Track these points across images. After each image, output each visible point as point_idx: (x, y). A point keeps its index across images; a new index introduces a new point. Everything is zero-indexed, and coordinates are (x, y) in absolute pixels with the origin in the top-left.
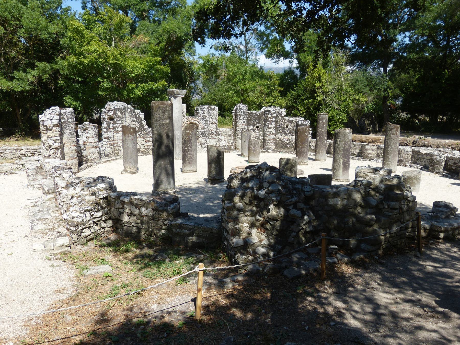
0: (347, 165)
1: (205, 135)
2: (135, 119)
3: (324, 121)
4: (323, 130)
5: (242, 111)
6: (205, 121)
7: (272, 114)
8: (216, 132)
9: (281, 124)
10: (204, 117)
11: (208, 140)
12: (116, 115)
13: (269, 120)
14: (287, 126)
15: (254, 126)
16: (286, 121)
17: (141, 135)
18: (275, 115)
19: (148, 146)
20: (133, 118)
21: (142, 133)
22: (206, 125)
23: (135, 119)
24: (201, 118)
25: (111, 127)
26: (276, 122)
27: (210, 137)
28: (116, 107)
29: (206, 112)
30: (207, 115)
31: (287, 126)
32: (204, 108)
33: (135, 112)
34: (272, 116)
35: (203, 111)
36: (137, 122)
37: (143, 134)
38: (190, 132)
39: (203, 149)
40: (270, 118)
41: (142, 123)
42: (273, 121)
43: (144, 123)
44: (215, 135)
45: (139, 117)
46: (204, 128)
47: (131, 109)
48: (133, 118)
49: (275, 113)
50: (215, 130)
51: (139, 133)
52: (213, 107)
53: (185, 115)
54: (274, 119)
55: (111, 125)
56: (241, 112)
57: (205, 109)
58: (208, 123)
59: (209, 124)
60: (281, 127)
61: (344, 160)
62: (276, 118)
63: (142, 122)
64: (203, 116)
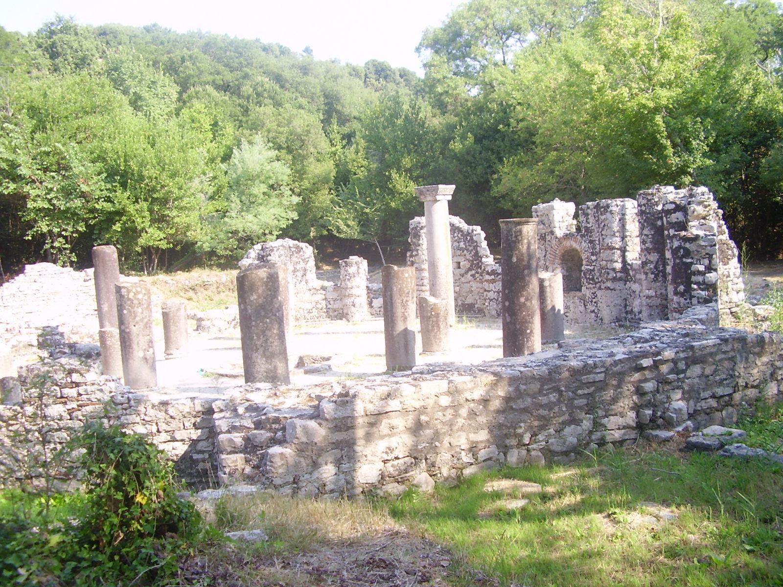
1: (593, 279)
2: (462, 245)
11: (599, 293)
17: (477, 275)
22: (593, 254)
23: (462, 245)
29: (591, 219)
32: (588, 208)
33: (462, 231)
36: (467, 250)
39: (588, 315)
44: (614, 279)
51: (473, 272)
52: (604, 202)
57: (589, 211)
64: (587, 229)
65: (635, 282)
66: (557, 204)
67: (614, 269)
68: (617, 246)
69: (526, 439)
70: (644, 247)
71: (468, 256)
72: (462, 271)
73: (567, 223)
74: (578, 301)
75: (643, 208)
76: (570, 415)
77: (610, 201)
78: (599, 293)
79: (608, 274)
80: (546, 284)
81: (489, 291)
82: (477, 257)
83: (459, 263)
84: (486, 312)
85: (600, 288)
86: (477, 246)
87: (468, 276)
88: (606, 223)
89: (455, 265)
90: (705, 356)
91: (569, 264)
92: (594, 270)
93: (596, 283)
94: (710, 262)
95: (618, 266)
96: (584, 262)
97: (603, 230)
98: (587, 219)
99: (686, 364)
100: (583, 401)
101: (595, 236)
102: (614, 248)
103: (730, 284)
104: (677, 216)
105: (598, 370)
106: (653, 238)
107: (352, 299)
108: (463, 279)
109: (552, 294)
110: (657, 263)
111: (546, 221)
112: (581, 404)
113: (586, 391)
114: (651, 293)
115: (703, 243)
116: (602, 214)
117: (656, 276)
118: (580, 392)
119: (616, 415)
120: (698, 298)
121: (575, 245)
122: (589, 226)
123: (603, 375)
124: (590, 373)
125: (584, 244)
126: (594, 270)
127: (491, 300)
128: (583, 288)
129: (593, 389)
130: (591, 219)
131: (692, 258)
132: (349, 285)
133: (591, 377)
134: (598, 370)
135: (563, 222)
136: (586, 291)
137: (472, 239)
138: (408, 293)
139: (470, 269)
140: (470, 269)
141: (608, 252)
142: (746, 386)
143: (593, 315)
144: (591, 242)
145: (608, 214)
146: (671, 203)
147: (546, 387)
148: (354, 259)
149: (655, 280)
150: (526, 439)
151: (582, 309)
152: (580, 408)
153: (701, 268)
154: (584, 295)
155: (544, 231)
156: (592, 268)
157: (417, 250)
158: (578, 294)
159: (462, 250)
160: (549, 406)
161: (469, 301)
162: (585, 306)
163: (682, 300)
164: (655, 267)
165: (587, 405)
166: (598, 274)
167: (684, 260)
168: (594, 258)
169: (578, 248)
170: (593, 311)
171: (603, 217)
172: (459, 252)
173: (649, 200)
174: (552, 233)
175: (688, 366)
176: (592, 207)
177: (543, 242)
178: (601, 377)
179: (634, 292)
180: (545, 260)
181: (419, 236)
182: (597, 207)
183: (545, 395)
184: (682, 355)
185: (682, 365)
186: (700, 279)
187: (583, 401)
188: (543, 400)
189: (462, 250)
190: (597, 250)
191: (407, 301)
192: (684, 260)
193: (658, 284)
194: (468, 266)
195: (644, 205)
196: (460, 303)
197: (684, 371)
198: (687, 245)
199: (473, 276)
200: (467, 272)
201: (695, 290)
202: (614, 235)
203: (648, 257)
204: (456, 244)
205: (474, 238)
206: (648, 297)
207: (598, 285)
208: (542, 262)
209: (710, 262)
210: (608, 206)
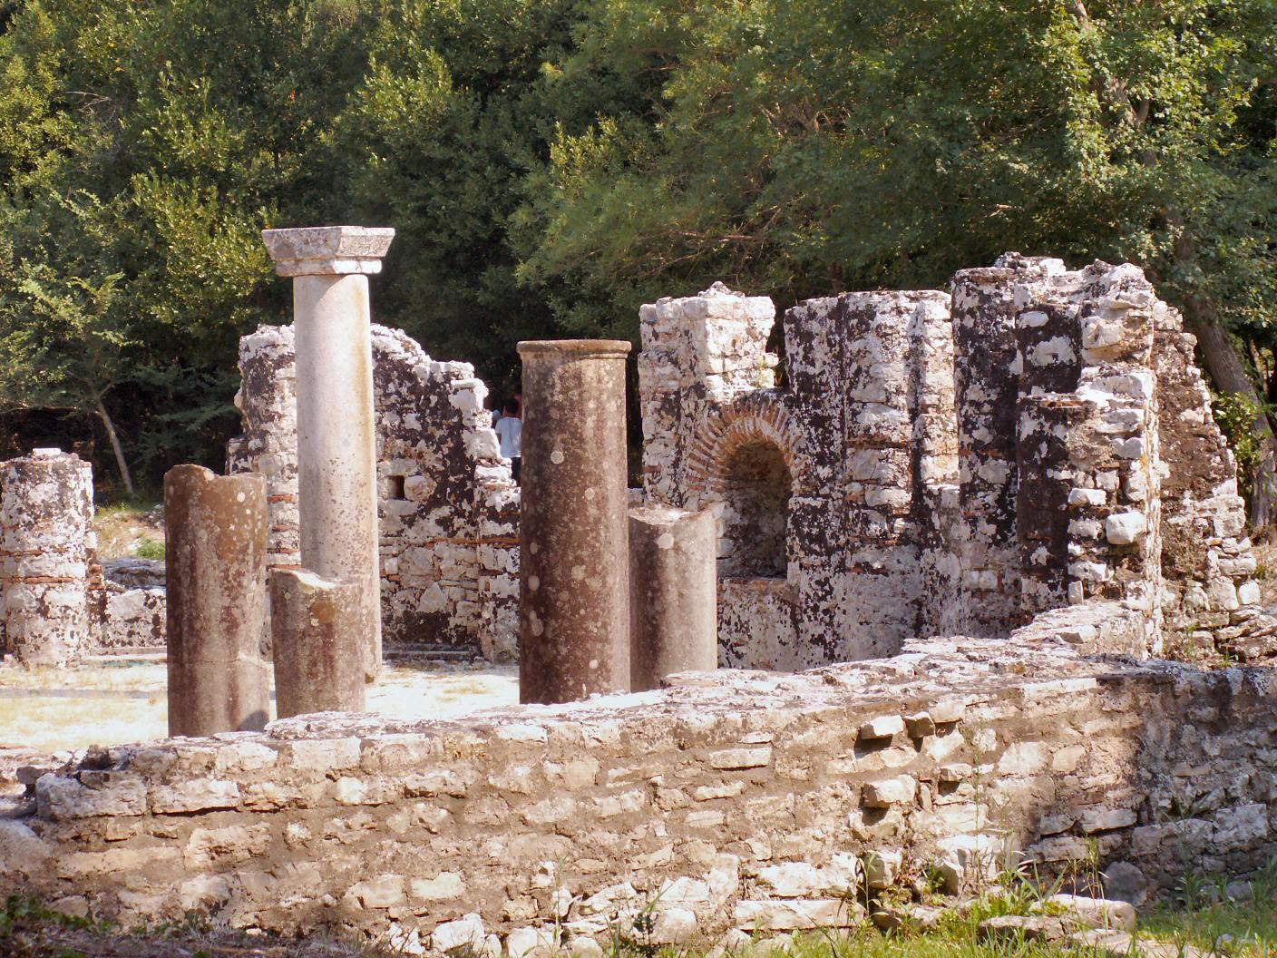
1: (820, 539)
2: (411, 421)
11: (839, 583)
17: (458, 522)
21: (460, 513)
22: (821, 460)
23: (411, 421)
29: (820, 352)
30: (830, 378)
32: (812, 315)
33: (412, 377)
36: (429, 438)
39: (803, 653)
45: (444, 408)
48: (400, 413)
51: (445, 511)
52: (858, 299)
57: (814, 326)
58: (837, 436)
64: (807, 382)
65: (946, 549)
66: (718, 298)
67: (885, 510)
68: (895, 438)
69: (562, 900)
70: (966, 439)
71: (432, 460)
72: (410, 507)
73: (747, 362)
74: (773, 608)
75: (969, 322)
76: (677, 849)
77: (876, 298)
78: (839, 583)
79: (867, 521)
80: (665, 542)
81: (494, 573)
82: (461, 462)
83: (399, 481)
84: (485, 640)
85: (841, 567)
86: (461, 426)
87: (430, 526)
88: (864, 363)
89: (387, 486)
90: (1054, 720)
91: (753, 492)
92: (824, 510)
93: (830, 552)
94: (1123, 481)
95: (900, 497)
96: (796, 486)
97: (853, 385)
98: (808, 350)
99: (999, 737)
100: (712, 818)
101: (832, 405)
102: (884, 443)
103: (1213, 556)
104: (1056, 349)
105: (752, 738)
106: (994, 413)
107: (40, 590)
108: (410, 533)
109: (682, 572)
110: (1006, 488)
111: (681, 352)
112: (706, 824)
113: (721, 791)
114: (988, 579)
115: (1104, 427)
116: (851, 336)
117: (1003, 527)
118: (703, 792)
119: (800, 859)
120: (1086, 583)
121: (768, 431)
122: (811, 370)
123: (767, 751)
124: (730, 742)
125: (796, 430)
126: (824, 510)
127: (501, 602)
128: (793, 567)
129: (738, 786)
130: (820, 352)
131: (1073, 468)
132: (32, 542)
133: (735, 756)
134: (752, 738)
135: (735, 356)
136: (800, 578)
137: (443, 403)
138: (244, 550)
139: (434, 502)
140: (434, 502)
141: (868, 454)
142: (1174, 811)
144: (818, 421)
145: (871, 336)
146: (1040, 308)
147: (613, 773)
148: (50, 455)
149: (999, 542)
150: (562, 900)
151: (786, 631)
152: (704, 833)
153: (1097, 498)
154: (794, 590)
155: (674, 386)
156: (818, 503)
157: (263, 435)
158: (775, 585)
160: (623, 824)
161: (432, 602)
163: (1043, 589)
164: (1000, 502)
165: (725, 826)
166: (835, 523)
167: (1050, 473)
169: (778, 439)
170: (819, 640)
171: (854, 346)
173: (985, 298)
174: (700, 389)
175: (1004, 743)
176: (822, 313)
177: (669, 419)
178: (762, 755)
179: (944, 580)
181: (272, 388)
182: (839, 313)
183: (610, 793)
184: (988, 713)
185: (986, 741)
186: (1092, 527)
187: (712, 818)
188: (609, 806)
190: (836, 448)
191: (239, 574)
192: (1050, 473)
193: (1008, 553)
195: (971, 312)
196: (399, 610)
197: (992, 757)
198: (1059, 431)
199: (444, 523)
200: (424, 511)
201: (1076, 559)
202: (887, 403)
203: (980, 469)
204: (390, 420)
205: (452, 399)
206: (979, 593)
207: (835, 559)
209: (1123, 481)
210: (870, 313)
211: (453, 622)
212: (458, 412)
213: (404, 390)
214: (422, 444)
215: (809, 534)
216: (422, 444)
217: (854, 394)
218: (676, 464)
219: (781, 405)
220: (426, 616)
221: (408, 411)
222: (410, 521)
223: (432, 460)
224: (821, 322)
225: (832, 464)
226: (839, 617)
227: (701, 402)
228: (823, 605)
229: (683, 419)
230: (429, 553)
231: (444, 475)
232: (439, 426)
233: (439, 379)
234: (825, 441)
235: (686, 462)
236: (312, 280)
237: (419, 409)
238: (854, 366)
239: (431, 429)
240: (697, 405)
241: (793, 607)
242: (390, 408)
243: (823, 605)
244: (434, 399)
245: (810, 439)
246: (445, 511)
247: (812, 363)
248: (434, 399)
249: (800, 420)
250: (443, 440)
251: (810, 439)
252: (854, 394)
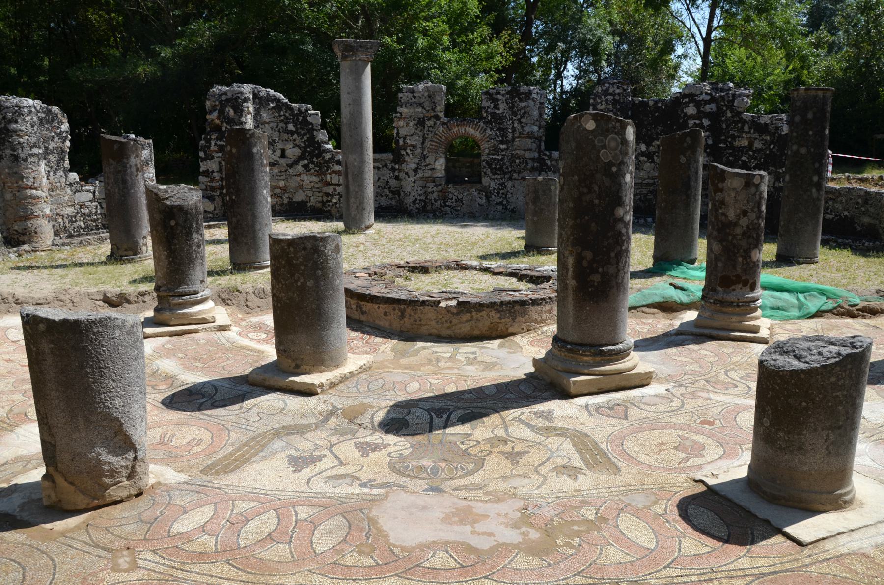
0: (596, 278)
1: (501, 169)
2: (291, 127)
3: (810, 116)
4: (803, 151)
5: (610, 97)
6: (499, 129)
7: (698, 104)
8: (533, 159)
9: (734, 138)
10: (497, 118)
11: (509, 184)
12: (224, 118)
13: (691, 122)
14: (751, 144)
15: (648, 145)
16: (746, 128)
17: (311, 166)
18: (710, 108)
19: (327, 195)
20: (286, 123)
21: (313, 163)
22: (502, 143)
23: (291, 127)
24: (486, 123)
25: (213, 148)
26: (715, 130)
27: (515, 175)
28: (224, 98)
29: (502, 106)
30: (507, 114)
31: (751, 144)
33: (292, 109)
34: (699, 111)
35: (495, 101)
36: (299, 134)
37: (318, 165)
38: (234, 151)
40: (692, 117)
41: (312, 138)
42: (701, 126)
43: (322, 135)
44: (533, 170)
45: (305, 122)
46: (496, 150)
47: (278, 100)
49: (713, 100)
50: (536, 155)
51: (306, 162)
53: (442, 115)
54: (706, 122)
55: (213, 144)
56: (607, 100)
57: (499, 97)
58: (510, 135)
59: (514, 138)
60: (732, 147)
61: (579, 260)
62: (713, 117)
63: (315, 133)
64: (494, 115)
78: (509, 184)
79: (527, 163)
85: (510, 178)
87: (299, 168)
93: (505, 173)
111: (427, 105)
122: (497, 112)
125: (489, 131)
126: (503, 159)
137: (305, 118)
143: (500, 207)
145: (531, 102)
151: (483, 201)
155: (422, 116)
156: (500, 157)
158: (478, 186)
159: (291, 133)
161: (299, 197)
162: (488, 198)
168: (503, 147)
170: (501, 203)
172: (286, 136)
173: (624, 90)
180: (423, 149)
181: (242, 111)
189: (291, 133)
194: (297, 152)
195: (619, 94)
196: (286, 201)
200: (296, 162)
205: (309, 118)
208: (419, 150)
210: (530, 92)
211: (309, 204)
212: (311, 124)
213: (287, 115)
214: (295, 136)
215: (495, 168)
216: (295, 136)
217: (523, 120)
218: (422, 144)
219: (481, 124)
220: (298, 203)
221: (289, 123)
222: (290, 166)
223: (297, 142)
224: (503, 95)
225: (507, 144)
226: (509, 196)
227: (438, 122)
228: (502, 192)
229: (426, 128)
230: (299, 178)
231: (305, 148)
232: (303, 129)
233: (303, 110)
234: (504, 136)
235: (428, 143)
236: (360, 63)
237: (293, 122)
238: (523, 111)
239: (300, 130)
240: (435, 123)
241: (486, 193)
242: (282, 121)
243: (502, 192)
244: (301, 118)
245: (496, 135)
246: (306, 162)
247: (499, 109)
248: (301, 118)
249: (491, 129)
250: (305, 134)
251: (496, 135)
252: (523, 120)
